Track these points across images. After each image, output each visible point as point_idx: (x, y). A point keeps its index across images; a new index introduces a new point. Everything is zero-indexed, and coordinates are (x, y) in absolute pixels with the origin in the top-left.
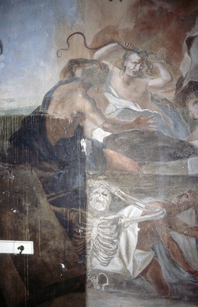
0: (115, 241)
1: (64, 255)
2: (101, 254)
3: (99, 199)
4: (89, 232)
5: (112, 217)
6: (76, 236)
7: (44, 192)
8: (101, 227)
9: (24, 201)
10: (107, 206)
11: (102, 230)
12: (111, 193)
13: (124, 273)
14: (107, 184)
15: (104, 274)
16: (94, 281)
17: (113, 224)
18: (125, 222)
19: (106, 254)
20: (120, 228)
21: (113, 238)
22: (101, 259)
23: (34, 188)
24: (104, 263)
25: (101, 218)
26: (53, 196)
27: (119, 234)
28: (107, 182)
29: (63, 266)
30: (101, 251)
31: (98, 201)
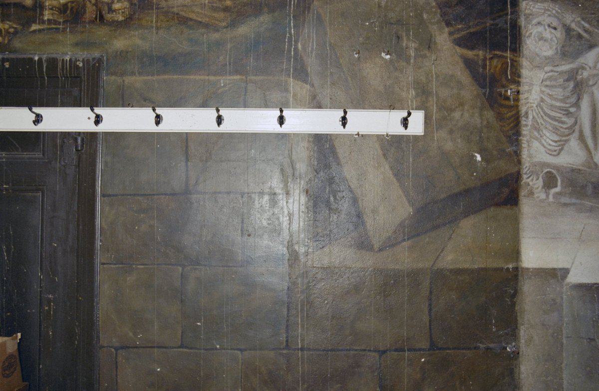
0: (572, 110)
1: (480, 137)
2: (548, 134)
3: (544, 35)
4: (526, 94)
5: (566, 67)
6: (503, 102)
7: (443, 24)
8: (546, 86)
9: (405, 38)
10: (556, 49)
11: (547, 90)
12: (564, 25)
13: (589, 168)
14: (557, 9)
15: (553, 171)
16: (536, 184)
17: (568, 80)
18: (590, 75)
19: (557, 134)
20: (580, 87)
21: (567, 105)
22: (547, 143)
23: (425, 16)
24: (552, 151)
25: (547, 69)
26: (459, 30)
27: (579, 99)
28: (557, 6)
29: (479, 158)
30: (546, 128)
31: (541, 39)
